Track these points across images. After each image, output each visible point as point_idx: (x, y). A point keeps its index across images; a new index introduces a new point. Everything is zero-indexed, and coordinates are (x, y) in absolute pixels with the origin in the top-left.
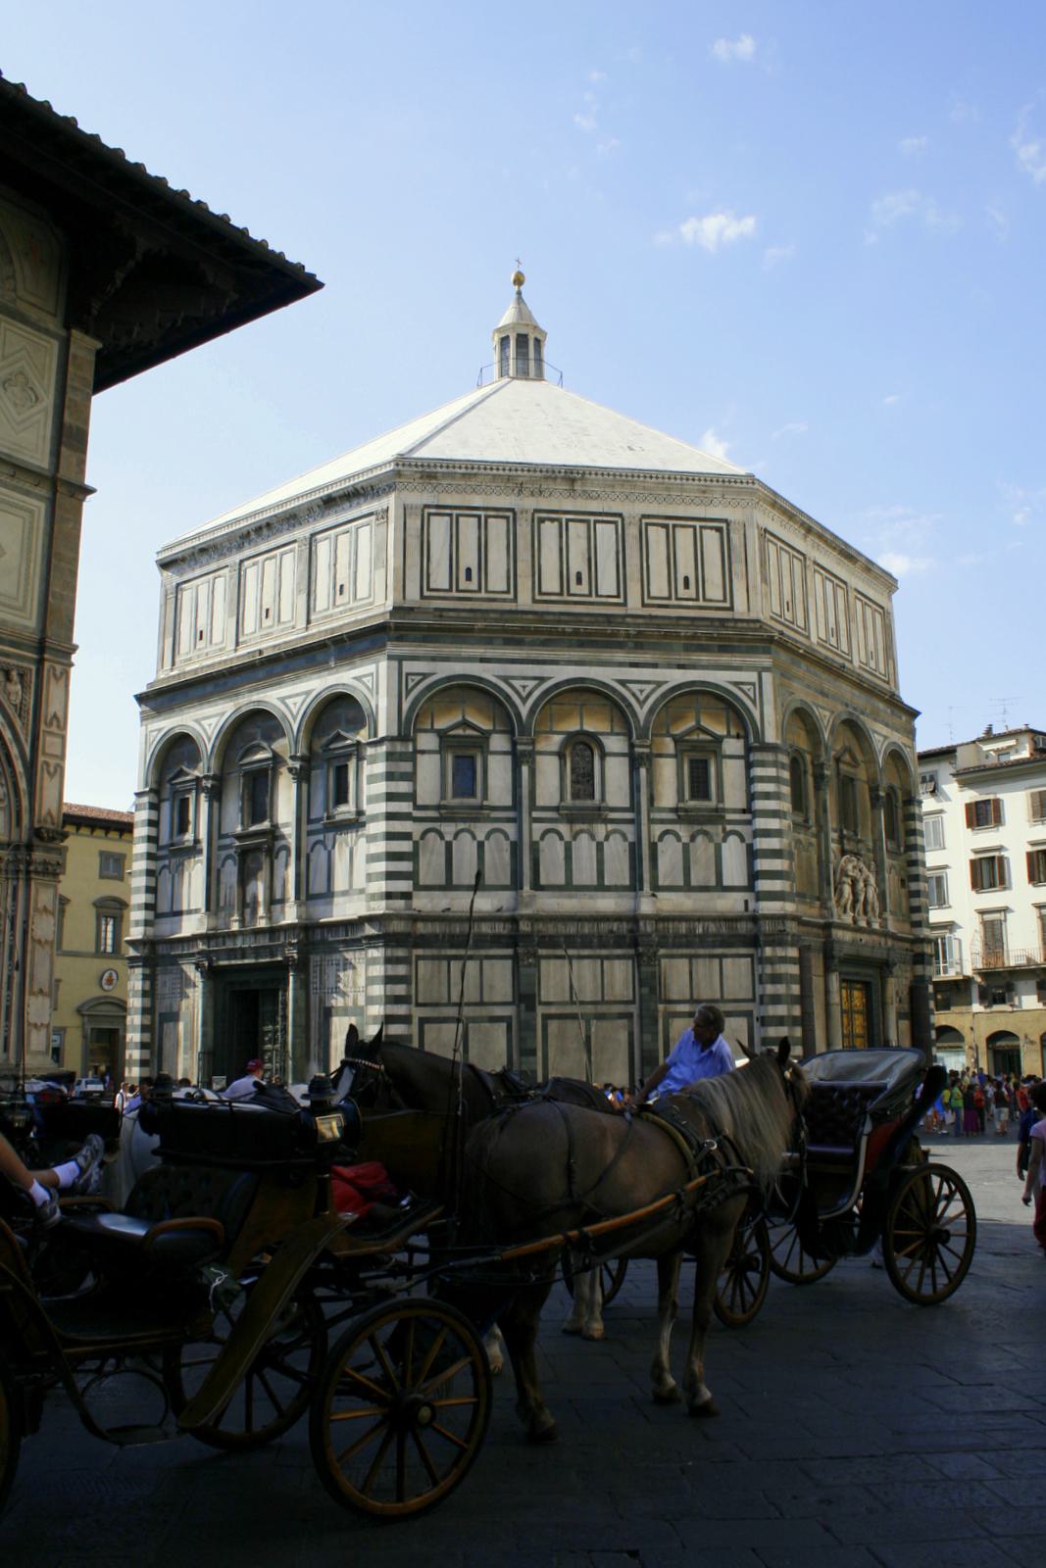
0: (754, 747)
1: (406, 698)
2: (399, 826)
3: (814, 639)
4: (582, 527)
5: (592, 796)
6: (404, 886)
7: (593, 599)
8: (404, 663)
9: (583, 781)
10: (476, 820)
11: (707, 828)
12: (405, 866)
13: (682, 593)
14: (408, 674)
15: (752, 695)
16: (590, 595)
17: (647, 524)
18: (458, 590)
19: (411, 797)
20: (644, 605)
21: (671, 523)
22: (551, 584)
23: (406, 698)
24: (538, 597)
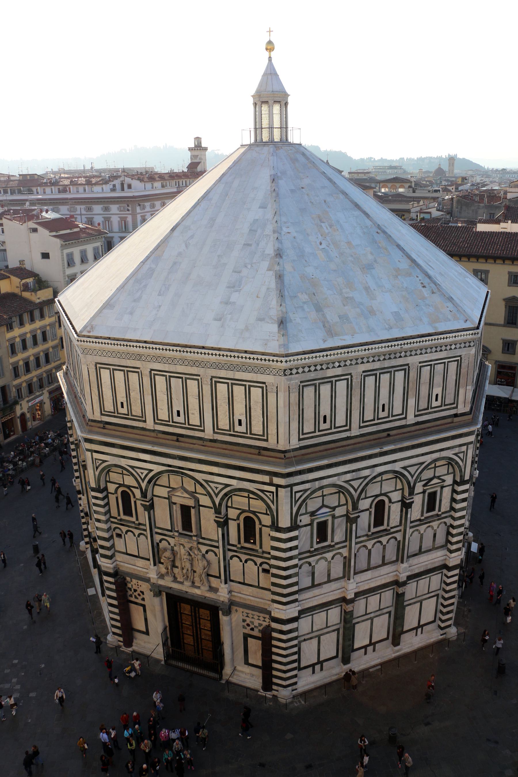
1: (295, 506)
5: (382, 524)
9: (379, 520)
10: (328, 552)
14: (296, 492)
22: (369, 415)
23: (295, 506)
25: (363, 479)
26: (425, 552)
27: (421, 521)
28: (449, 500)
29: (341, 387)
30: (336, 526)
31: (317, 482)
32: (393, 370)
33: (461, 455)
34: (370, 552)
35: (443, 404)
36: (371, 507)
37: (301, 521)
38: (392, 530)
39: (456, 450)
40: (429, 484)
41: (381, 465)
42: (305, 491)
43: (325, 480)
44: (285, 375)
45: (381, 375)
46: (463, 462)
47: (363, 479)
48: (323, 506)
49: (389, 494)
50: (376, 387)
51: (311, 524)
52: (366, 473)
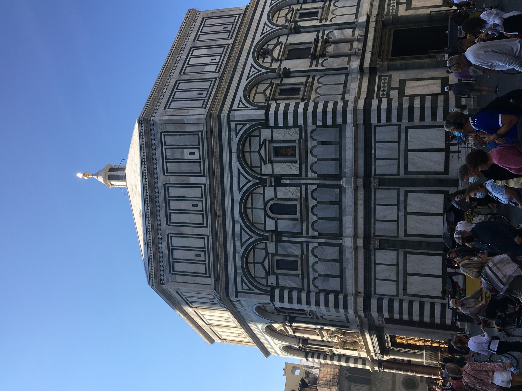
0: (265, 123)
2: (313, 300)
3: (216, 75)
4: (171, 202)
5: (295, 206)
6: (341, 297)
7: (204, 199)
8: (238, 290)
10: (308, 260)
11: (309, 150)
12: (332, 297)
13: (197, 156)
14: (243, 289)
15: (242, 126)
16: (202, 201)
17: (167, 172)
18: (205, 261)
19: (300, 290)
20: (204, 176)
21: (165, 161)
22: (198, 218)
23: (253, 290)
24: (205, 225)
25: (243, 231)
26: (341, 153)
27: (303, 162)
28: (288, 130)
29: (177, 242)
30: (284, 253)
31: (238, 271)
32: (168, 198)
33: (239, 127)
34: (320, 218)
35: (196, 147)
36: (273, 219)
37: (271, 283)
38: (304, 196)
39: (233, 134)
40: (264, 158)
41: (233, 214)
42: (243, 281)
43: (237, 264)
44: (164, 284)
45: (171, 208)
46: (246, 124)
47: (243, 231)
48: (262, 264)
49: (267, 199)
50: (179, 213)
51: (277, 275)
52: (237, 228)
